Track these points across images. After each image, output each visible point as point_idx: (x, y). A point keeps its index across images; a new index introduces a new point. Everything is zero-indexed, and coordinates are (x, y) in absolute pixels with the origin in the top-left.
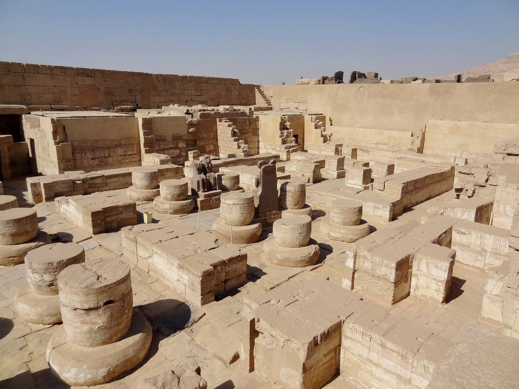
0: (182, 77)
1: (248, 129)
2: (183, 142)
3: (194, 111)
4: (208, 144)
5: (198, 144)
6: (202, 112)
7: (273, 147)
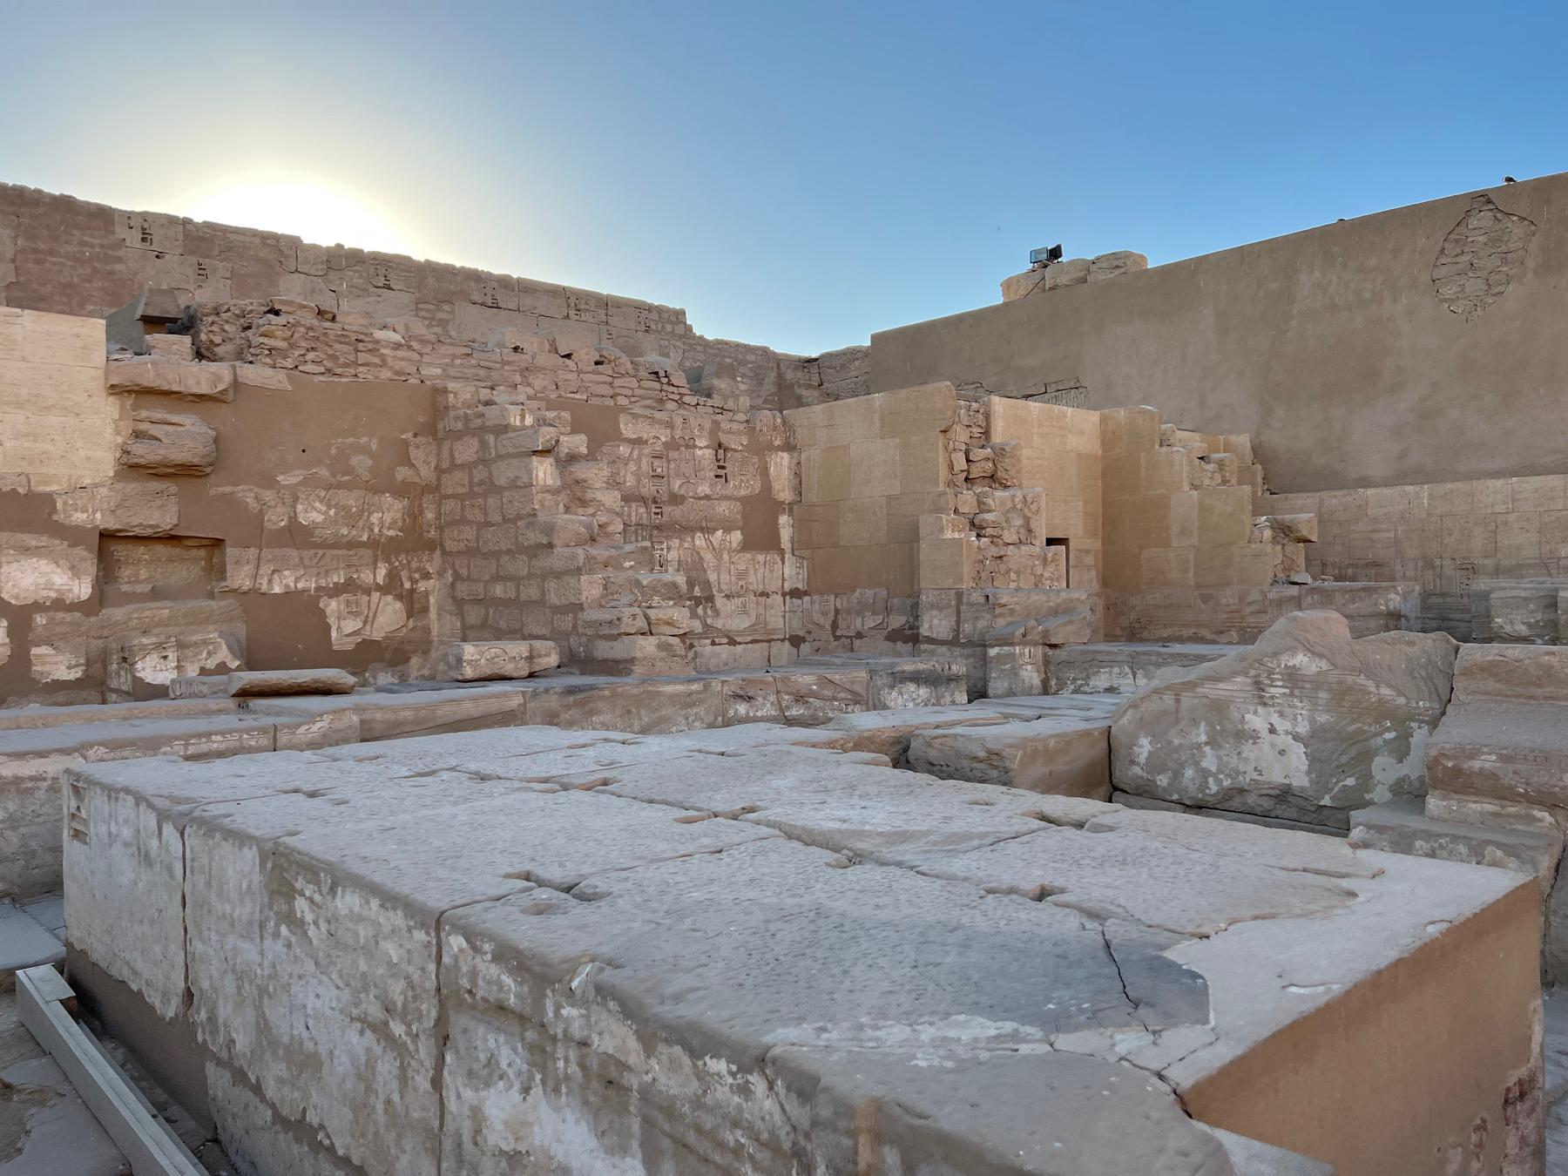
1: (707, 497)
2: (36, 552)
4: (349, 586)
5: (240, 578)
7: (897, 621)
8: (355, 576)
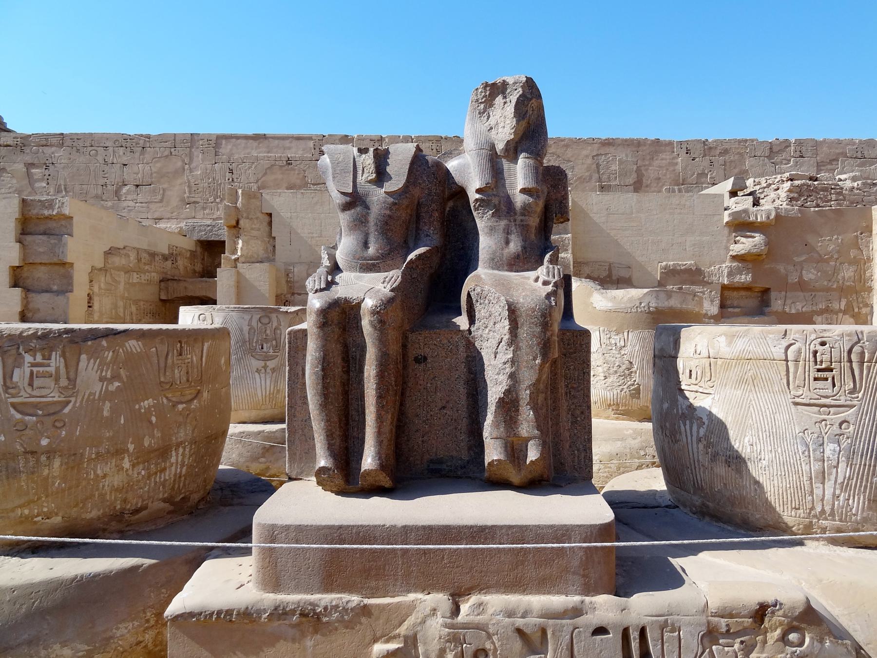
0: (770, 143)
3: (765, 185)
6: (797, 183)
8: (830, 305)
